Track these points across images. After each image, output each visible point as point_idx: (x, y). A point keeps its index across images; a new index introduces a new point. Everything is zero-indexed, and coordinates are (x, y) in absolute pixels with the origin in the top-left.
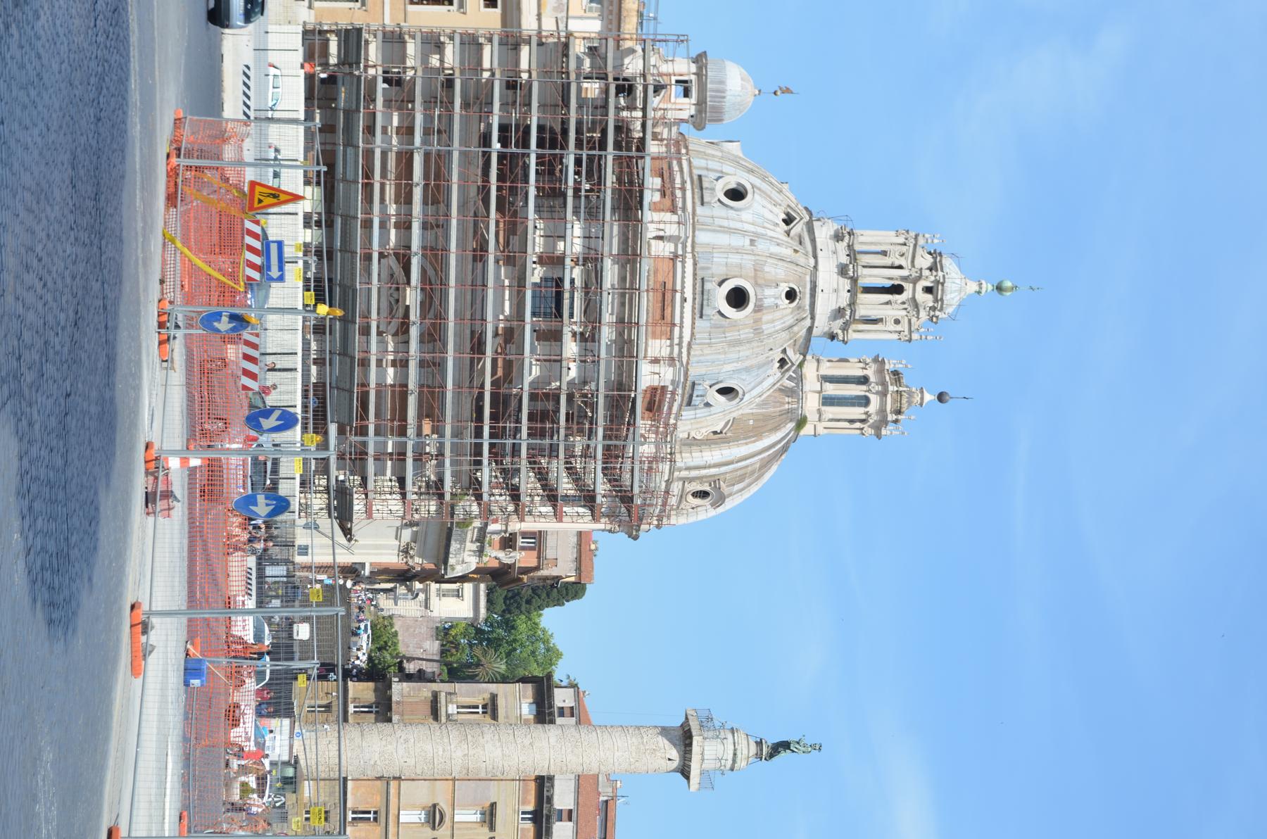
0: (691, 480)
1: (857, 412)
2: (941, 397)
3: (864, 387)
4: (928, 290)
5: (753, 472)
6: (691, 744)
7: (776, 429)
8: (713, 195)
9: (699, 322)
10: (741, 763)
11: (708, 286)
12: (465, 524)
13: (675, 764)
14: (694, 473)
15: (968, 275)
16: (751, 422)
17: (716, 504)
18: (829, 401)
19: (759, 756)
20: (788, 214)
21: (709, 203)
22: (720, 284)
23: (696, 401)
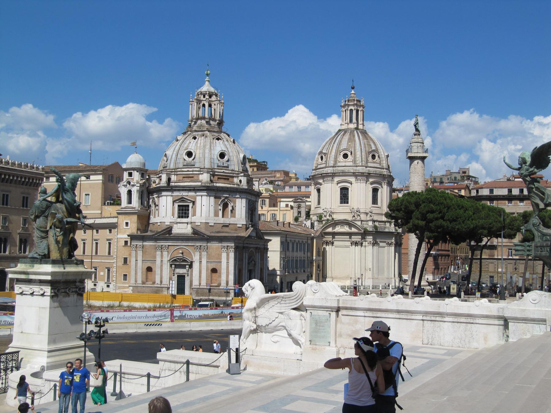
2: (353, 88)
4: (204, 97)
5: (368, 142)
6: (412, 157)
7: (354, 136)
9: (196, 166)
10: (420, 140)
11: (185, 164)
12: (375, 227)
13: (420, 162)
15: (203, 84)
17: (378, 152)
18: (351, 121)
19: (419, 135)
22: (185, 160)
23: (225, 165)
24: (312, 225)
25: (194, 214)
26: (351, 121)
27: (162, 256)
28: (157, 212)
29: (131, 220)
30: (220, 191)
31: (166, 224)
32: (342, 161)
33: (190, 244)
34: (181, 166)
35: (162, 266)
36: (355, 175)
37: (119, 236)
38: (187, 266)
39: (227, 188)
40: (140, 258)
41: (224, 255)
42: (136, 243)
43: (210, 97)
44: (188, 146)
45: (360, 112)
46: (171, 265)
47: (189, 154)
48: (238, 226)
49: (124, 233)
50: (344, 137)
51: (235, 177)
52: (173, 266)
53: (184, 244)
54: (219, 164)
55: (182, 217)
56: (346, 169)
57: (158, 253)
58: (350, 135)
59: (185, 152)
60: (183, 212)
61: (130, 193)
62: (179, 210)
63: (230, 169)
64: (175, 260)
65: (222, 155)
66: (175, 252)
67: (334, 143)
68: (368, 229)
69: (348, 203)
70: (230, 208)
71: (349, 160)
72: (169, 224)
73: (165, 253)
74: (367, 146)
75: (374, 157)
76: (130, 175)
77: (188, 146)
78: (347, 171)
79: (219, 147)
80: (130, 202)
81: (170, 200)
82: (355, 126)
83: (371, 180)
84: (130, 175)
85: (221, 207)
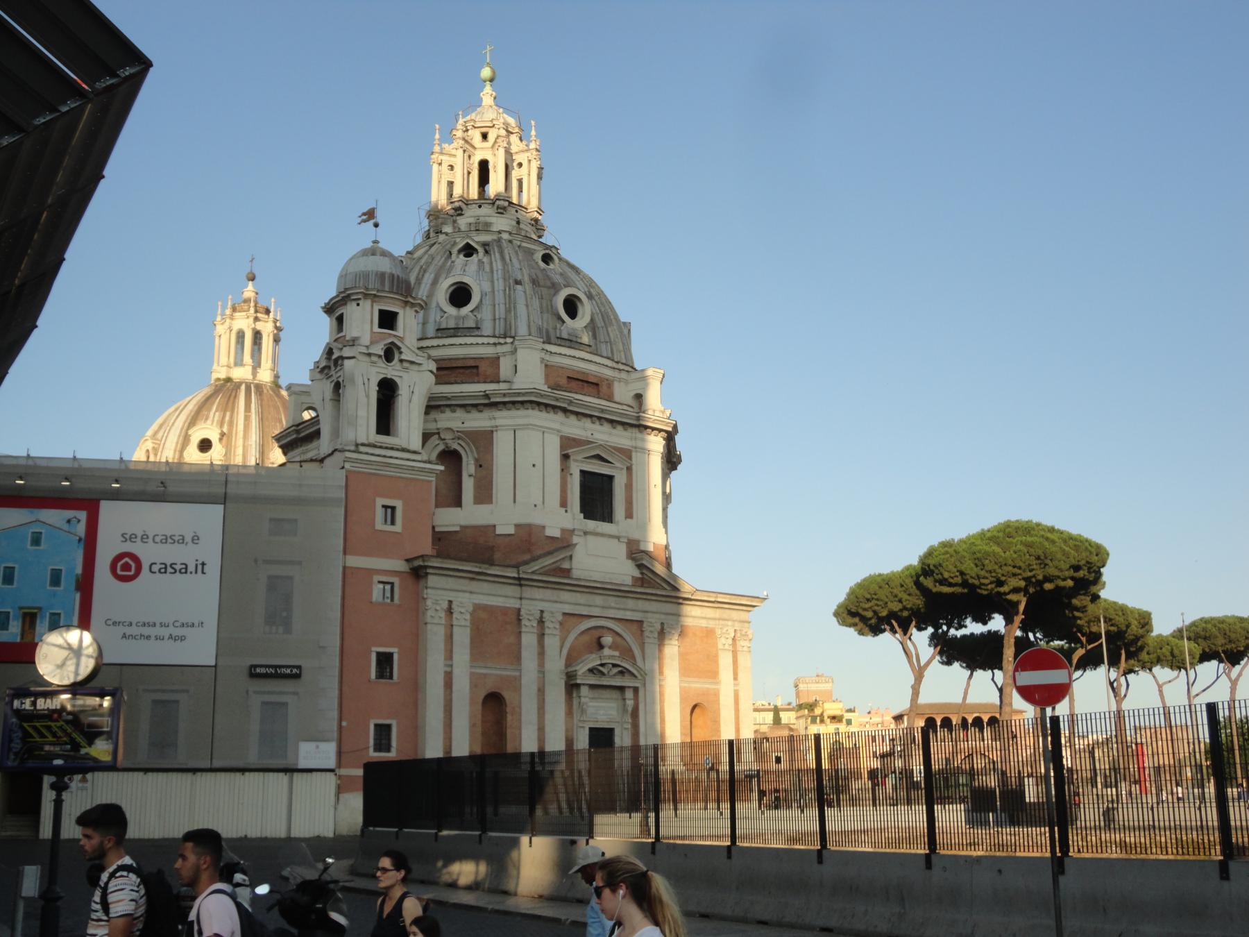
1: (267, 342)
2: (252, 278)
8: (464, 318)
11: (565, 335)
20: (460, 251)
21: (477, 322)
22: (564, 322)
25: (629, 515)
27: (541, 653)
28: (468, 485)
31: (549, 532)
33: (629, 615)
35: (541, 691)
37: (354, 561)
38: (629, 694)
41: (725, 661)
42: (451, 596)
46: (572, 687)
52: (584, 691)
53: (611, 613)
61: (387, 391)
64: (591, 670)
72: (557, 534)
73: (552, 642)
76: (388, 320)
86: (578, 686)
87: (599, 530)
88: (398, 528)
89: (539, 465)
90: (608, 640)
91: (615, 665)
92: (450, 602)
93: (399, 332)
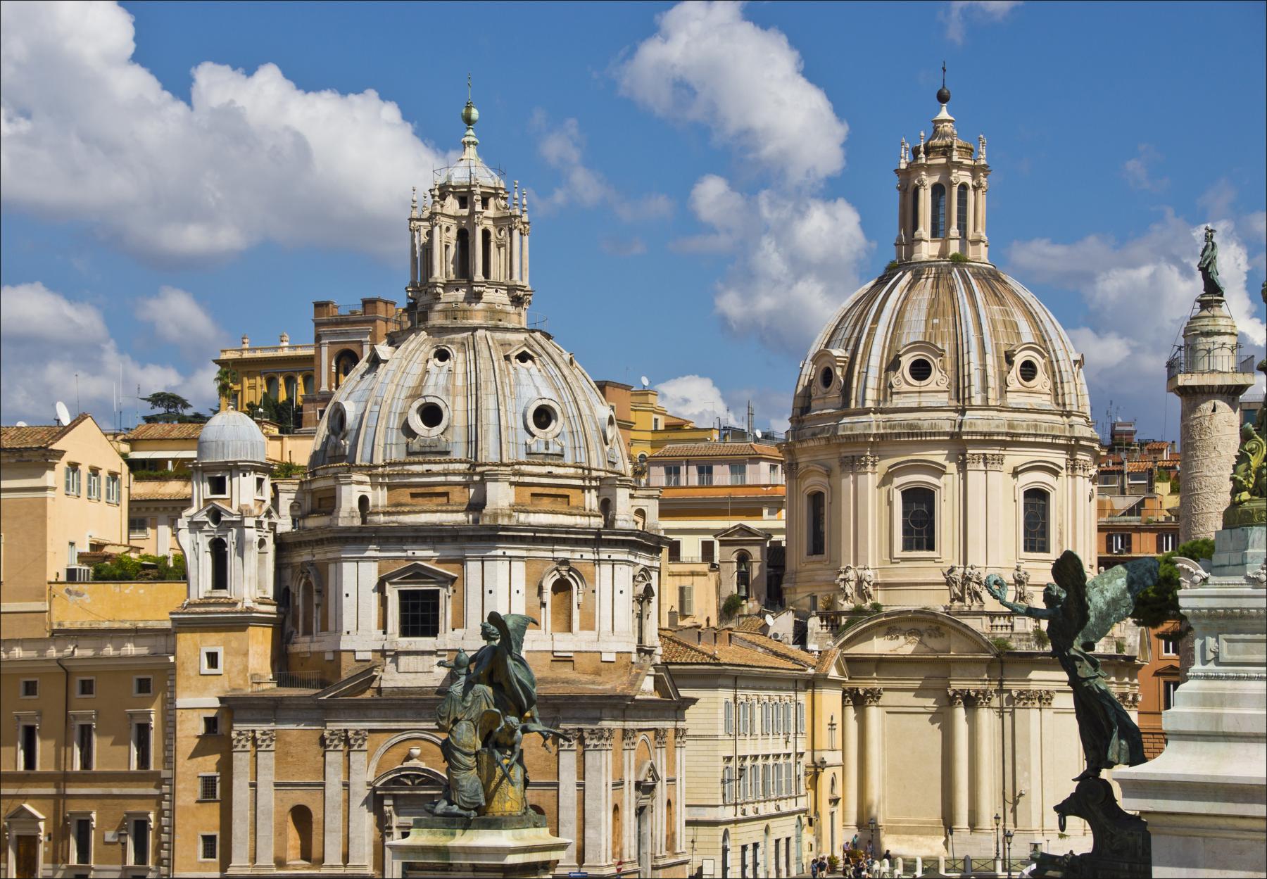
0: (1004, 386)
3: (922, 191)
7: (952, 290)
11: (416, 446)
14: (993, 382)
16: (936, 321)
23: (555, 449)
24: (801, 636)
25: (459, 622)
26: (938, 231)
28: (317, 614)
29: (226, 644)
30: (544, 541)
32: (905, 388)
34: (397, 454)
36: (958, 444)
39: (568, 529)
40: (267, 779)
41: (568, 760)
43: (485, 203)
44: (421, 384)
45: (971, 193)
47: (431, 414)
48: (605, 657)
49: (203, 690)
50: (914, 296)
51: (590, 488)
54: (534, 449)
55: (415, 633)
56: (925, 420)
57: (335, 758)
58: (936, 286)
59: (416, 404)
60: (420, 615)
62: (403, 608)
63: (568, 459)
64: (394, 781)
65: (544, 416)
66: (389, 756)
67: (876, 320)
68: (1013, 644)
69: (931, 547)
70: (576, 598)
71: (933, 387)
72: (369, 656)
73: (357, 759)
74: (1001, 328)
75: (1028, 370)
76: (218, 486)
77: (421, 384)
78: (926, 427)
79: (533, 385)
80: (220, 580)
81: (371, 573)
82: (954, 248)
83: (1016, 457)
84: (218, 486)
85: (548, 596)
86: (382, 797)
87: (413, 648)
88: (220, 670)
89: (353, 595)
90: (416, 751)
91: (419, 776)
92: (254, 731)
93: (227, 496)
